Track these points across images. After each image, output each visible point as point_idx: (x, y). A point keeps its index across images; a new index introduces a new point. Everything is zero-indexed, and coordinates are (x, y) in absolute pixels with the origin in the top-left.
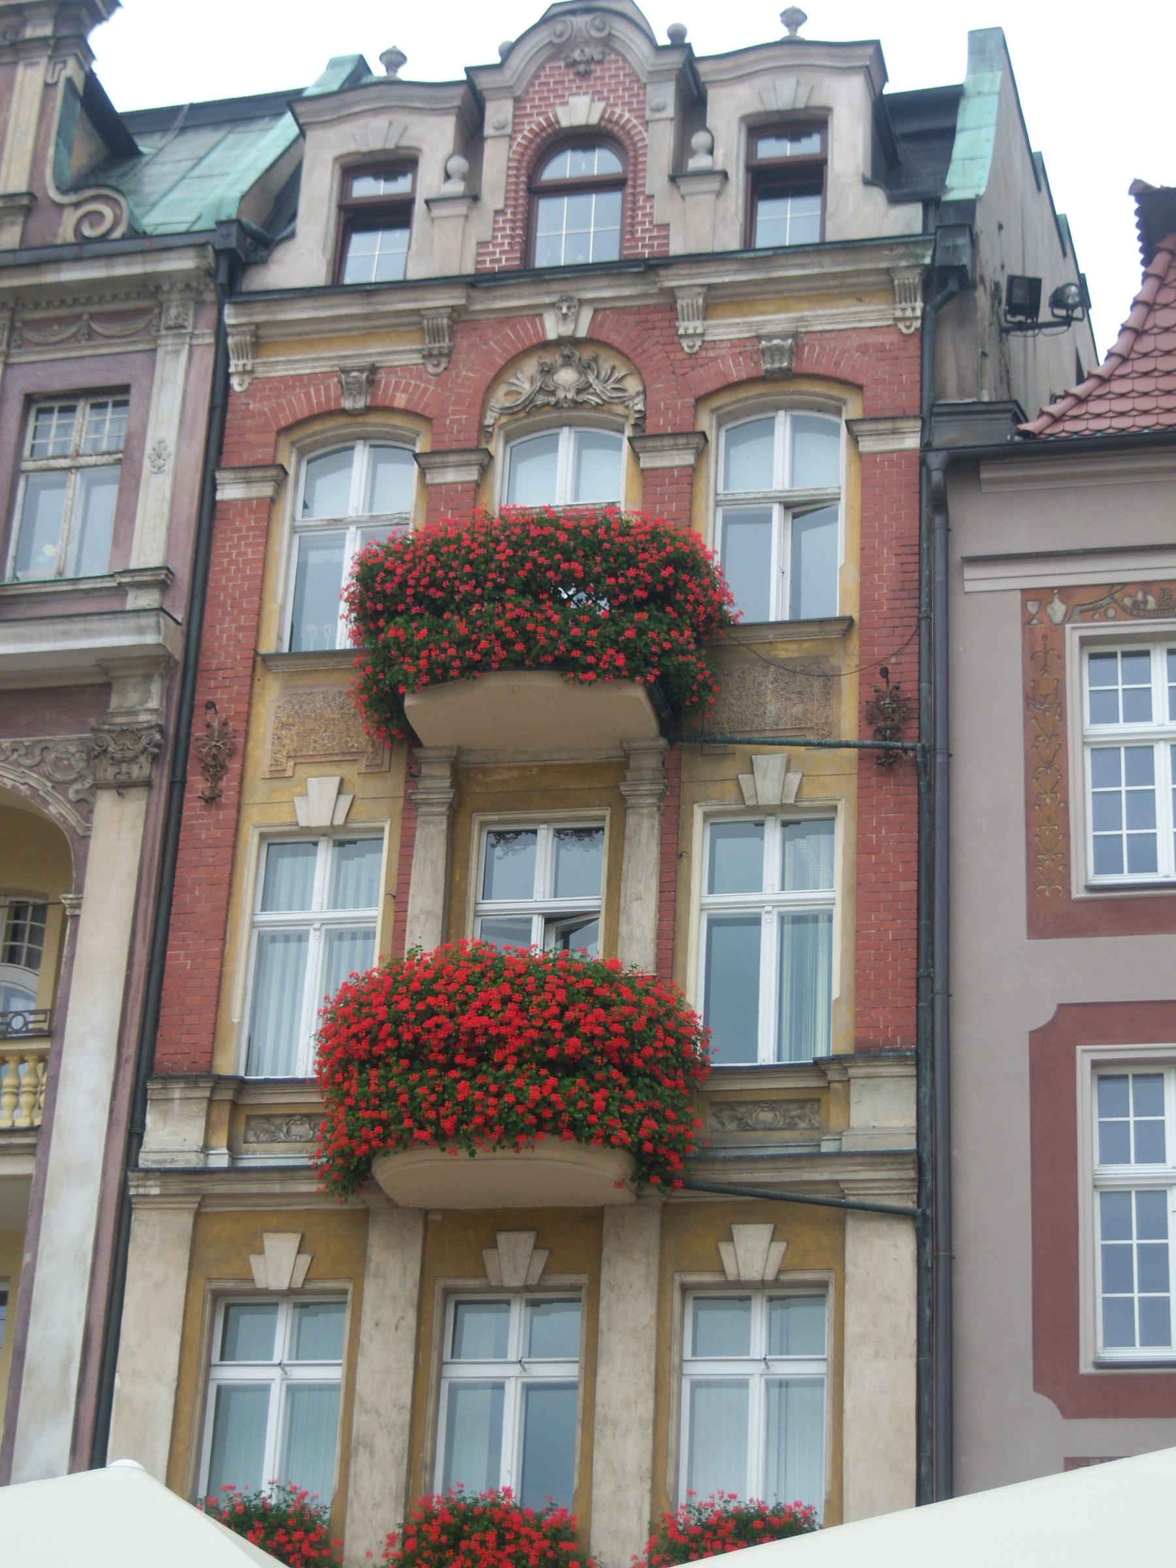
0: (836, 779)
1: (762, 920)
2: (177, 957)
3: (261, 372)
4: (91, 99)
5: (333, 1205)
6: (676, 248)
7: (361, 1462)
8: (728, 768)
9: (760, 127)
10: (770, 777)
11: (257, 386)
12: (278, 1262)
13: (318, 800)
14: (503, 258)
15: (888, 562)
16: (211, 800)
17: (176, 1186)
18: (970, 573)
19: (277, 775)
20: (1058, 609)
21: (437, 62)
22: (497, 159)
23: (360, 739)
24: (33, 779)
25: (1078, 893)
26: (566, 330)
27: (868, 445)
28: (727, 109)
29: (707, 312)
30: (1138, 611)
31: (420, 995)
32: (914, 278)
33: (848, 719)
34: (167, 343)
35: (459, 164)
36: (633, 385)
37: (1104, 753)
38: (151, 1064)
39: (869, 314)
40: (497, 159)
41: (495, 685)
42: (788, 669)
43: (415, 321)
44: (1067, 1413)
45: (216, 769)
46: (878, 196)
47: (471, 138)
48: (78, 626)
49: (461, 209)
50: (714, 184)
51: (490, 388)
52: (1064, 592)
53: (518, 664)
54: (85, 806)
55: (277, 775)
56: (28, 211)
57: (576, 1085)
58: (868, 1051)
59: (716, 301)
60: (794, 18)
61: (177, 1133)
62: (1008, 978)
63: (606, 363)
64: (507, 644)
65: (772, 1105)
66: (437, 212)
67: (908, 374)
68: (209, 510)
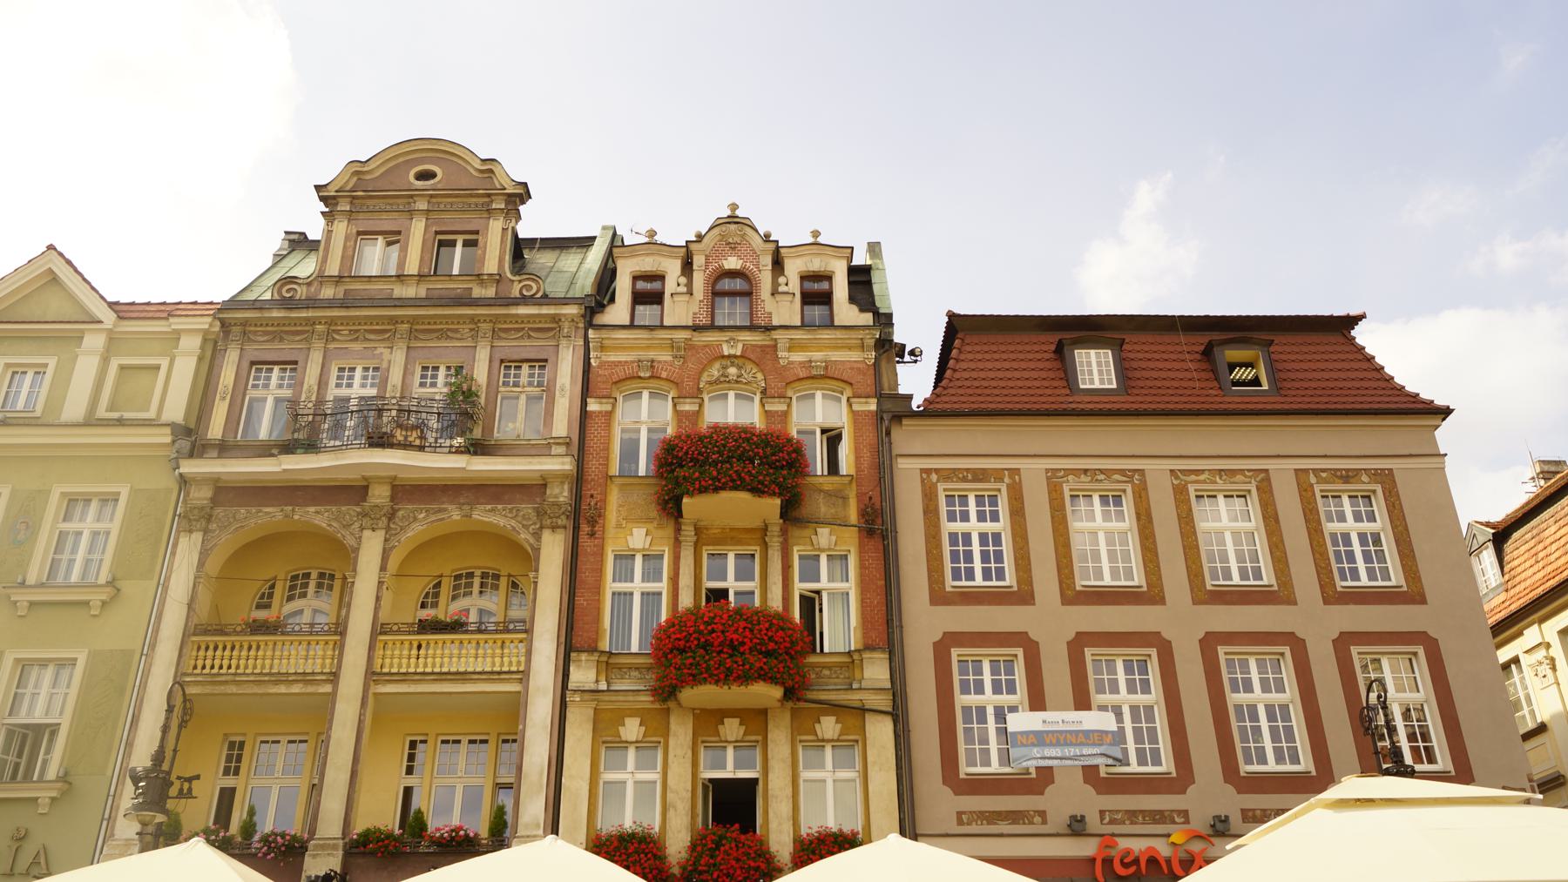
0: (849, 541)
2: (580, 601)
3: (604, 358)
4: (515, 235)
5: (657, 706)
6: (775, 322)
7: (671, 813)
8: (807, 532)
9: (805, 278)
11: (602, 365)
12: (632, 729)
13: (638, 538)
14: (705, 321)
15: (866, 454)
16: (592, 535)
17: (587, 696)
18: (900, 460)
19: (619, 526)
20: (934, 477)
21: (676, 234)
22: (699, 279)
23: (654, 513)
24: (513, 523)
25: (948, 589)
26: (732, 352)
27: (856, 407)
28: (793, 268)
29: (790, 349)
30: (964, 480)
31: (709, 624)
32: (872, 342)
33: (853, 515)
34: (563, 342)
35: (683, 280)
36: (760, 376)
37: (953, 537)
38: (573, 642)
39: (855, 356)
40: (699, 279)
41: (725, 495)
42: (828, 494)
43: (672, 345)
44: (956, 793)
45: (593, 522)
46: (855, 308)
47: (687, 267)
48: (536, 459)
49: (686, 297)
50: (789, 298)
51: (701, 373)
52: (937, 471)
53: (736, 489)
54: (537, 535)
55: (619, 526)
56: (498, 282)
57: (772, 661)
58: (868, 647)
59: (793, 346)
60: (816, 234)
61: (583, 674)
62: (924, 624)
63: (749, 366)
64: (732, 480)
65: (830, 668)
66: (676, 298)
67: (870, 380)
68: (584, 414)
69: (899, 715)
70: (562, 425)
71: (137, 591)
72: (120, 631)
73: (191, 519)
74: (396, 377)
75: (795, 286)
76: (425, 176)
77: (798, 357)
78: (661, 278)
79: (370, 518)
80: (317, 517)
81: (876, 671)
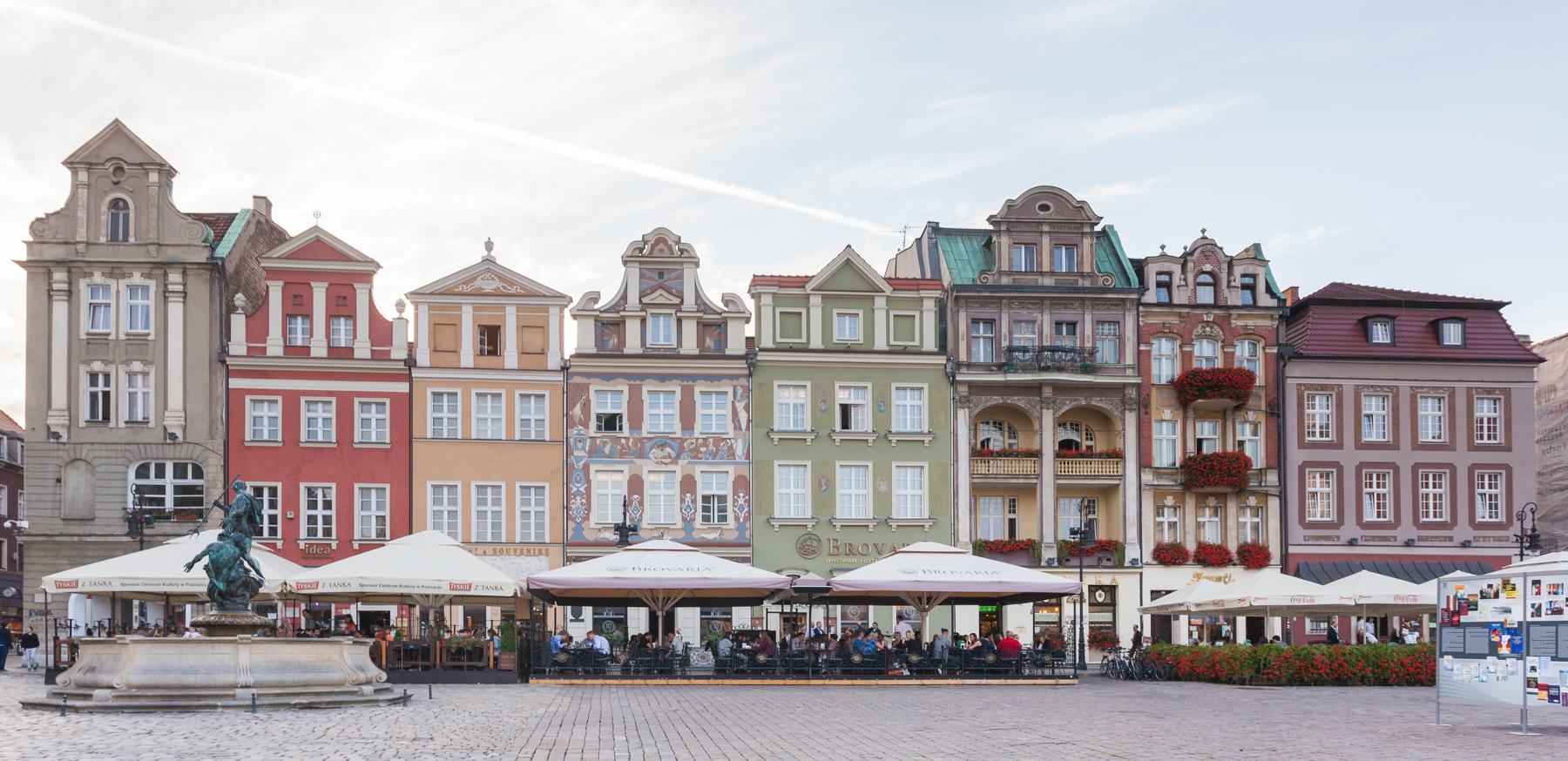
22: (1190, 277)
59: (1240, 316)
68: (1139, 352)
70: (1130, 359)
73: (960, 402)
74: (1047, 330)
77: (1241, 323)
78: (1170, 274)
79: (1045, 403)
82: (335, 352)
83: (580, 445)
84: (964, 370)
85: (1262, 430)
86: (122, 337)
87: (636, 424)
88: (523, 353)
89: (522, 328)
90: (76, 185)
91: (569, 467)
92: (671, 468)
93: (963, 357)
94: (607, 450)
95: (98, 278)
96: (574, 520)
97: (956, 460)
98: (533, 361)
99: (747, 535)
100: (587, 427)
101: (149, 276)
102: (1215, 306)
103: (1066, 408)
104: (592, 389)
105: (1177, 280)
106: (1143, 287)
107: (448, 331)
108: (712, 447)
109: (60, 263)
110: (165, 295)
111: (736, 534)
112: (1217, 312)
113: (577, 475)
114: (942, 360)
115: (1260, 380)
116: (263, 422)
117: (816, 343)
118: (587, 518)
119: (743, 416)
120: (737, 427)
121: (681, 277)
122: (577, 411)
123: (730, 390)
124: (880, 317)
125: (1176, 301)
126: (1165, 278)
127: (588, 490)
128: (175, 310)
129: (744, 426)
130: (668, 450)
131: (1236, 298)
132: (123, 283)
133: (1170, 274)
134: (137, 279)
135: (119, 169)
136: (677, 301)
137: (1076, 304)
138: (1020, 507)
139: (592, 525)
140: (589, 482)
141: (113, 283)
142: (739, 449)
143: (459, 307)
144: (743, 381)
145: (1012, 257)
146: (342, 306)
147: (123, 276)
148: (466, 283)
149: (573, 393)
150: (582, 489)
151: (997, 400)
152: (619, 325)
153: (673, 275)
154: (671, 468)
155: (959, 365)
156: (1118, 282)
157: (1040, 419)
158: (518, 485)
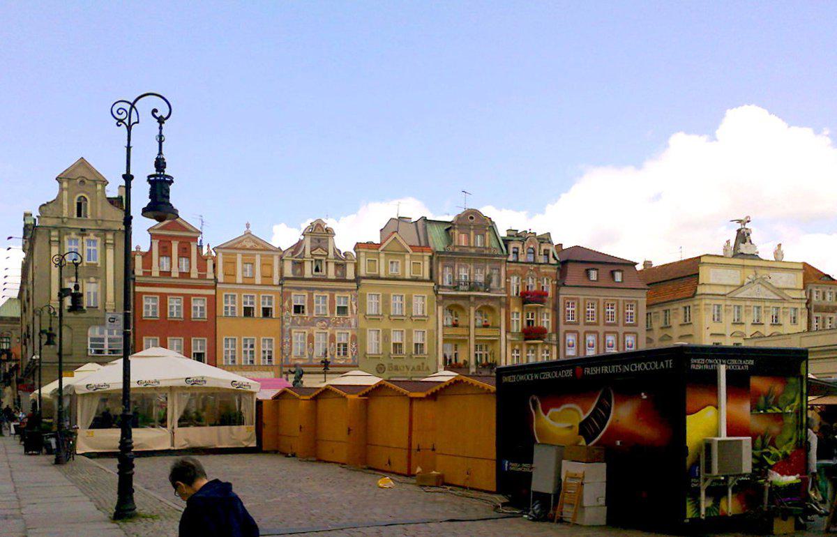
1: (545, 321)
10: (547, 310)
13: (516, 310)
43: (521, 267)
61: (508, 337)
62: (563, 328)
69: (558, 346)
70: (503, 286)
71: (433, 319)
72: (431, 324)
73: (439, 303)
75: (542, 253)
76: (472, 218)
77: (543, 271)
78: (518, 248)
79: (473, 304)
80: (460, 303)
81: (554, 337)
82: (182, 275)
83: (288, 320)
84: (440, 289)
85: (550, 316)
86: (85, 265)
87: (311, 311)
88: (263, 277)
89: (263, 265)
90: (62, 189)
91: (282, 331)
92: (326, 331)
93: (440, 284)
94: (299, 323)
95: (73, 235)
96: (285, 354)
97: (437, 329)
98: (267, 281)
99: (356, 361)
100: (290, 311)
101: (96, 236)
102: (534, 263)
103: (479, 306)
104: (293, 294)
105: (520, 252)
106: (508, 255)
107: (231, 266)
108: (342, 322)
109: (55, 228)
110: (105, 245)
111: (352, 361)
112: (535, 266)
113: (287, 334)
114: (433, 284)
115: (550, 295)
116: (149, 307)
117: (383, 275)
118: (290, 354)
119: (354, 308)
120: (352, 313)
121: (327, 242)
122: (286, 304)
123: (349, 296)
124: (407, 263)
125: (520, 260)
126: (515, 250)
127: (291, 341)
128: (110, 253)
129: (355, 312)
130: (324, 323)
131: (542, 259)
132: (85, 238)
133: (518, 248)
134: (92, 237)
135: (82, 182)
136: (326, 253)
137: (483, 261)
138: (459, 348)
139: (293, 357)
140: (291, 337)
141: (80, 238)
142: (353, 324)
143: (236, 254)
144: (354, 292)
145: (461, 239)
146: (185, 252)
147: (85, 235)
148: (239, 243)
149: (284, 296)
150: (288, 340)
151: (453, 302)
152: (301, 264)
153: (324, 241)
154: (326, 331)
155: (439, 286)
156: (499, 252)
157: (469, 311)
158: (262, 338)
